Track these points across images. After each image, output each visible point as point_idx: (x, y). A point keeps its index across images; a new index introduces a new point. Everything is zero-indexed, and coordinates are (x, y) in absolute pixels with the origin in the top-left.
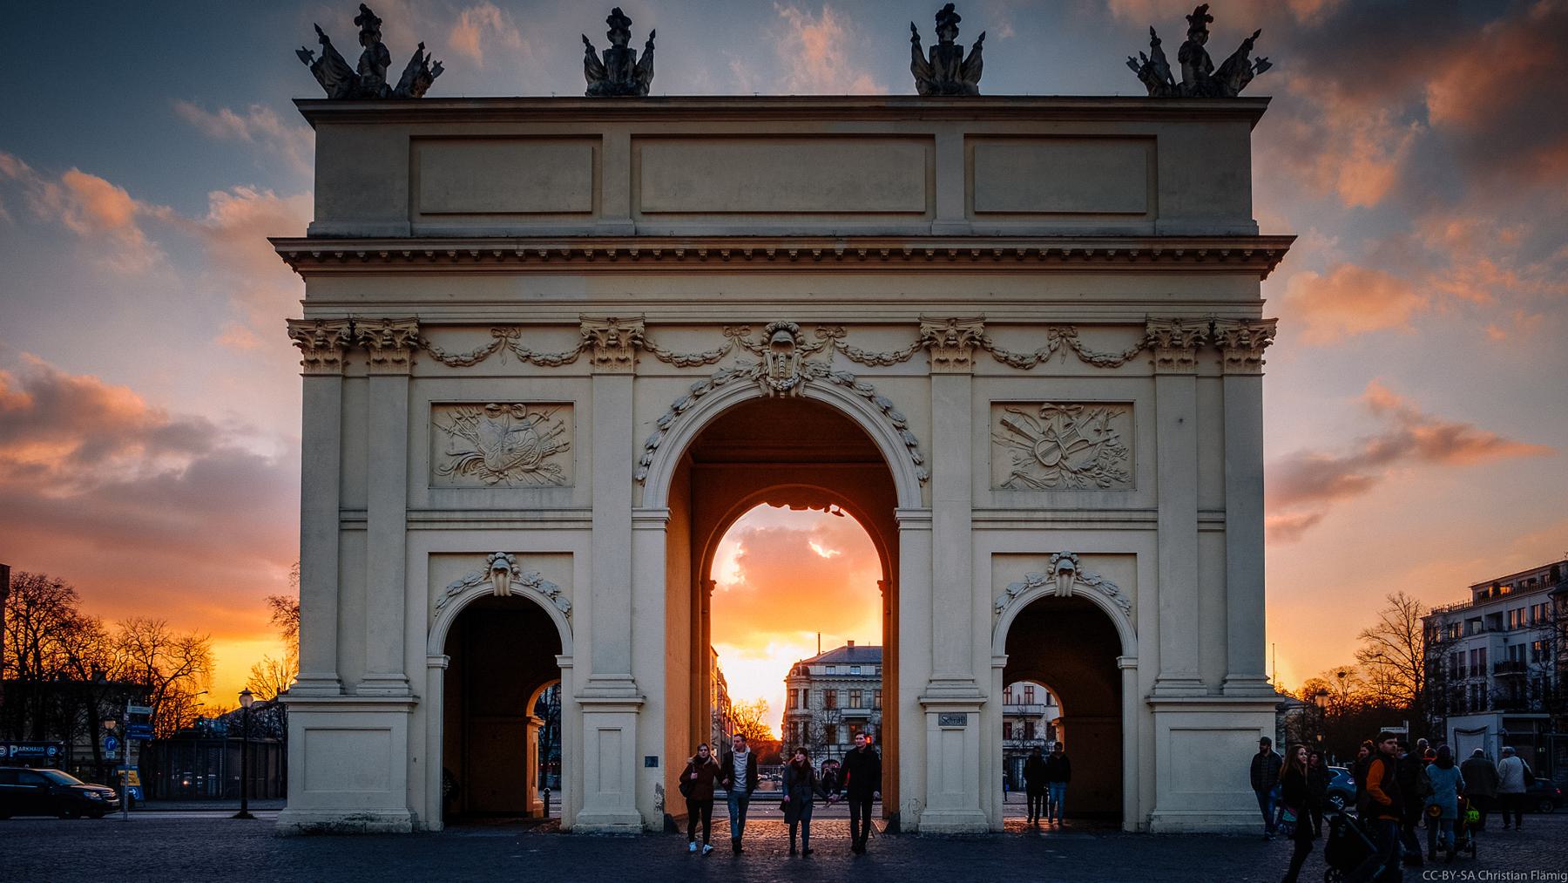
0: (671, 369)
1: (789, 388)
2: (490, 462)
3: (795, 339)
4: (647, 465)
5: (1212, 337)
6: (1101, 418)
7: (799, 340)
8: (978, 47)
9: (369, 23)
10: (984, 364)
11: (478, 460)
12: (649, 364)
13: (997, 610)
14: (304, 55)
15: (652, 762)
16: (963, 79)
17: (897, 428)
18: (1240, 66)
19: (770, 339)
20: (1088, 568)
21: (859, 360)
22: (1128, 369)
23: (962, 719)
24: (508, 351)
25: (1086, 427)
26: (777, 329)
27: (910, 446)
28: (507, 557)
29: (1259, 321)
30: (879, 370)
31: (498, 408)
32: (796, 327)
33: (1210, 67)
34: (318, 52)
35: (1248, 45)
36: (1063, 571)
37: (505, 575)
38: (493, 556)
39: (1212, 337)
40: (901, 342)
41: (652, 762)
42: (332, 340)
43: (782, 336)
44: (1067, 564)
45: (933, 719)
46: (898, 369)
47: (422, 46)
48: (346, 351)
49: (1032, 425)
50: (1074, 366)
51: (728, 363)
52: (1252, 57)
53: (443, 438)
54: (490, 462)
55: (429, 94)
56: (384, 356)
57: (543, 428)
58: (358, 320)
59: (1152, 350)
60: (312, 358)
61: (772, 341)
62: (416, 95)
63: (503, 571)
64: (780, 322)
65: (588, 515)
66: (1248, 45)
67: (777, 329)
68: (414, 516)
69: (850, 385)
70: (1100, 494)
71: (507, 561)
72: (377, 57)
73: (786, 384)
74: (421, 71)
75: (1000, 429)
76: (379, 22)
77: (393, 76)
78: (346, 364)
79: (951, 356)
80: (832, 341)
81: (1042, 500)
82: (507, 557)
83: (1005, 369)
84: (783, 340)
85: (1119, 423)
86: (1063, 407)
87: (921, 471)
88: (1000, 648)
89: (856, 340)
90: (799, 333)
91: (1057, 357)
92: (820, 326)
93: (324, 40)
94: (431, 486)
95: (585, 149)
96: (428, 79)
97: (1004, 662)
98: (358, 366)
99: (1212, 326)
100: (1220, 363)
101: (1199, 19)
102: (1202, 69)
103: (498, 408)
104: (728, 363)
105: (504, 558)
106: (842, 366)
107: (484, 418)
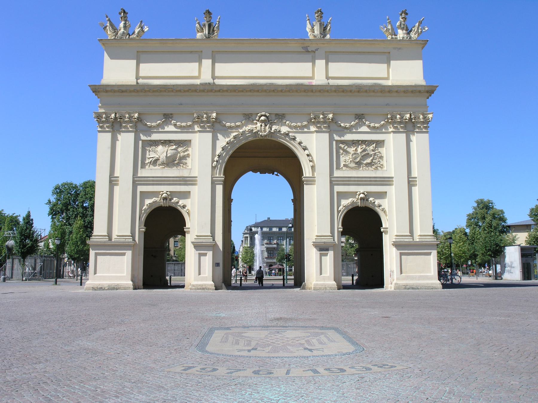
1: (266, 135)
2: (161, 160)
3: (268, 119)
6: (374, 145)
7: (269, 119)
11: (158, 160)
13: (338, 212)
17: (303, 149)
19: (259, 119)
28: (167, 193)
36: (361, 199)
37: (167, 199)
38: (162, 192)
44: (362, 196)
57: (180, 149)
61: (260, 119)
67: (262, 116)
71: (167, 194)
73: (265, 134)
80: (281, 120)
82: (167, 193)
86: (360, 142)
88: (340, 226)
90: (269, 117)
105: (166, 193)
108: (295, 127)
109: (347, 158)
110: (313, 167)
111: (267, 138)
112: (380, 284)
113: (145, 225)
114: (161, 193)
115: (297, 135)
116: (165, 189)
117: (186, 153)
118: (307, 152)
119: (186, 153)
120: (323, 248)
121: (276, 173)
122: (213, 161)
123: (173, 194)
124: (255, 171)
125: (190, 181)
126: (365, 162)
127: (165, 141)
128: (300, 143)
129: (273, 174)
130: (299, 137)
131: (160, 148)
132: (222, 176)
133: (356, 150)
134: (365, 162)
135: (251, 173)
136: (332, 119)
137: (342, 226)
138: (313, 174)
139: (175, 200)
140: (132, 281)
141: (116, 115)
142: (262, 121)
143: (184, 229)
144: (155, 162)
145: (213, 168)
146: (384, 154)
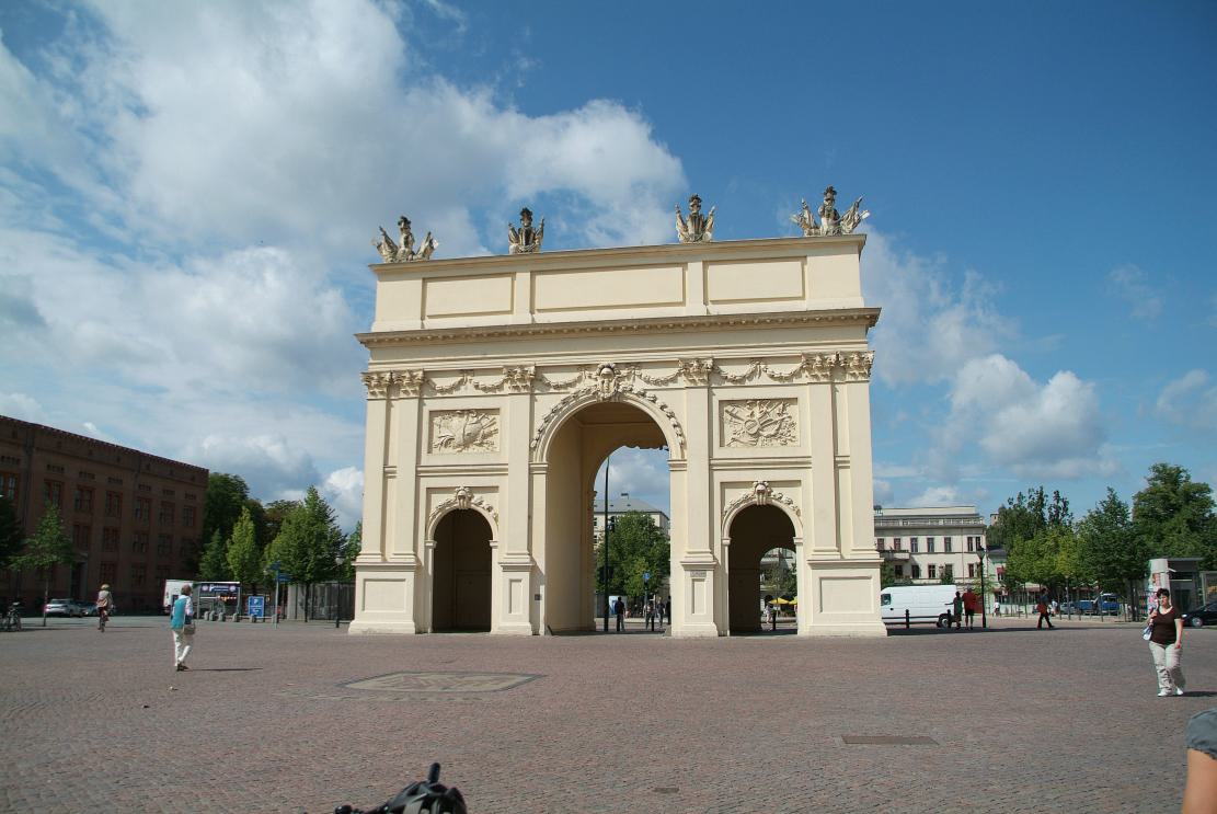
1: (610, 398)
2: (457, 441)
21: (648, 382)
25: (774, 413)
27: (675, 426)
31: (463, 412)
36: (759, 492)
40: (671, 372)
43: (605, 371)
44: (760, 487)
49: (744, 412)
51: (580, 387)
53: (436, 428)
57: (485, 422)
62: (425, 259)
64: (606, 363)
68: (419, 469)
69: (643, 395)
73: (607, 395)
85: (791, 410)
88: (726, 535)
89: (645, 372)
92: (628, 365)
103: (463, 412)
104: (580, 387)
106: (639, 386)
108: (656, 382)
109: (738, 428)
110: (683, 445)
111: (613, 401)
112: (488, 629)
113: (436, 538)
115: (657, 394)
116: (463, 482)
117: (492, 429)
118: (673, 421)
119: (492, 429)
120: (696, 569)
122: (531, 440)
123: (473, 490)
124: (631, 445)
125: (500, 470)
126: (765, 434)
128: (662, 408)
130: (663, 398)
131: (456, 421)
132: (545, 461)
133: (752, 414)
134: (765, 434)
136: (712, 368)
137: (730, 536)
138: (683, 456)
139: (477, 497)
140: (415, 621)
142: (605, 376)
144: (448, 442)
145: (532, 450)
146: (796, 419)
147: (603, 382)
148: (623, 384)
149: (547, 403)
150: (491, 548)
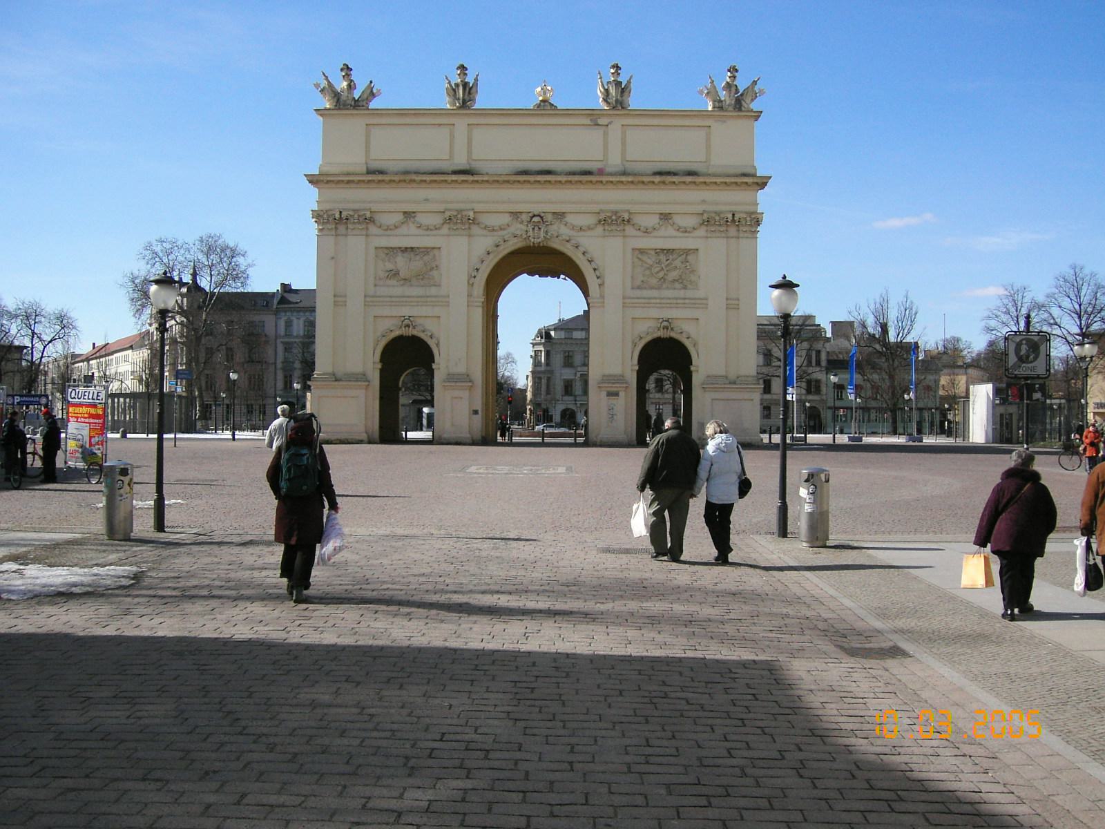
0: (485, 232)
4: (475, 277)
5: (733, 220)
6: (684, 256)
8: (629, 82)
9: (347, 69)
10: (629, 230)
12: (475, 230)
14: (317, 86)
15: (476, 412)
16: (622, 97)
18: (752, 91)
20: (675, 324)
22: (697, 233)
23: (617, 394)
24: (411, 224)
26: (534, 216)
27: (595, 269)
29: (756, 213)
30: (581, 233)
32: (542, 215)
33: (737, 91)
34: (324, 84)
35: (755, 83)
39: (733, 220)
41: (476, 412)
42: (330, 219)
44: (665, 324)
45: (604, 393)
46: (589, 233)
47: (371, 82)
48: (336, 224)
50: (671, 231)
51: (512, 230)
52: (756, 88)
54: (402, 274)
55: (373, 105)
56: (354, 226)
58: (344, 209)
59: (707, 225)
60: (320, 227)
63: (408, 326)
65: (447, 300)
66: (755, 83)
67: (534, 216)
70: (682, 291)
72: (351, 86)
73: (539, 240)
74: (371, 94)
75: (636, 260)
76: (351, 70)
77: (357, 94)
78: (336, 228)
79: (614, 227)
81: (655, 293)
83: (639, 233)
84: (538, 219)
87: (599, 281)
88: (636, 361)
91: (663, 228)
93: (327, 78)
94: (375, 285)
95: (446, 130)
96: (373, 95)
97: (637, 368)
98: (342, 229)
99: (733, 215)
100: (738, 231)
101: (733, 70)
102: (732, 94)
104: (512, 230)
106: (565, 231)
107: (400, 254)
111: (541, 245)
113: (382, 360)
114: (403, 319)
121: (562, 276)
124: (531, 274)
127: (406, 248)
129: (559, 278)
135: (524, 278)
141: (340, 215)
143: (431, 366)
147: (533, 229)
148: (553, 229)
149: (483, 243)
150: (433, 370)
